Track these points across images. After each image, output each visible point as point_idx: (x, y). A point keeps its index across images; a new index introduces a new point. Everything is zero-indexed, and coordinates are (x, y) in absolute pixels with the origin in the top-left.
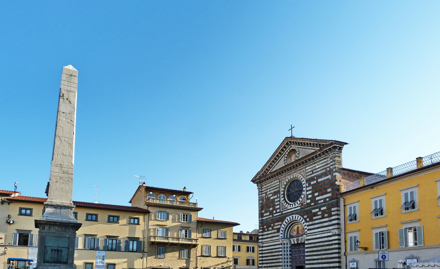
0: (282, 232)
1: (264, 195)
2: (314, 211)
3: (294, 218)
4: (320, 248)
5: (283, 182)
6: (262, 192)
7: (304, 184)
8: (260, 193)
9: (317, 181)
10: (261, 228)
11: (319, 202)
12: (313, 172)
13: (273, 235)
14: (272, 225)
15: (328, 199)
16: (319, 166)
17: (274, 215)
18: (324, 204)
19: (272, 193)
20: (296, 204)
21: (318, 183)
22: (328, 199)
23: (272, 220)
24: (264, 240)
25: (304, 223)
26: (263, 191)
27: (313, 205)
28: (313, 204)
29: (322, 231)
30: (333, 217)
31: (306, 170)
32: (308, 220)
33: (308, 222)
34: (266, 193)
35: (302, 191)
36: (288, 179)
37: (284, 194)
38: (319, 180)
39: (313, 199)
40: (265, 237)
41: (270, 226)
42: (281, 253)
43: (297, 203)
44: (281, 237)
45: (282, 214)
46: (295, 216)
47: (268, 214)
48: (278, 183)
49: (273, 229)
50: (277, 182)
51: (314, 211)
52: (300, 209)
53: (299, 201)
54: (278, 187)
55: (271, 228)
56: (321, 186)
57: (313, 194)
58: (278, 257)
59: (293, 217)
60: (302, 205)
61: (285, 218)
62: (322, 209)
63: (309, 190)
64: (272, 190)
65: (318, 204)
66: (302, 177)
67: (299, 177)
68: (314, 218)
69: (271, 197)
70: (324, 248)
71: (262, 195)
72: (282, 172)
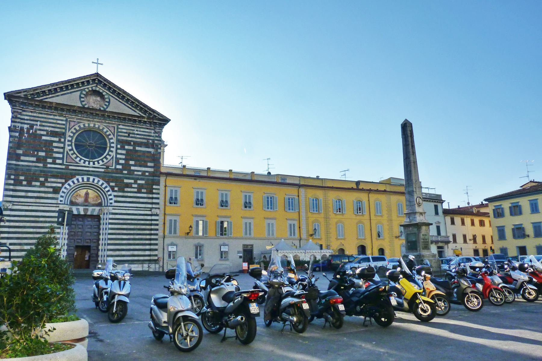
0: (63, 195)
1: (26, 126)
4: (132, 227)
5: (72, 124)
8: (14, 119)
9: (134, 148)
10: (12, 177)
11: (136, 173)
12: (129, 135)
15: (147, 174)
16: (140, 132)
17: (49, 166)
18: (142, 177)
20: (96, 163)
22: (147, 174)
23: (41, 171)
25: (109, 191)
27: (126, 174)
28: (125, 172)
30: (155, 196)
31: (118, 128)
33: (116, 191)
34: (32, 126)
36: (84, 125)
38: (137, 148)
40: (23, 194)
43: (99, 163)
44: (61, 201)
45: (67, 168)
46: (94, 180)
47: (34, 159)
49: (42, 185)
52: (104, 172)
56: (139, 156)
59: (88, 179)
60: (107, 167)
61: (72, 176)
62: (139, 182)
64: (49, 127)
65: (133, 174)
68: (126, 189)
69: (44, 135)
70: (138, 227)
71: (23, 125)
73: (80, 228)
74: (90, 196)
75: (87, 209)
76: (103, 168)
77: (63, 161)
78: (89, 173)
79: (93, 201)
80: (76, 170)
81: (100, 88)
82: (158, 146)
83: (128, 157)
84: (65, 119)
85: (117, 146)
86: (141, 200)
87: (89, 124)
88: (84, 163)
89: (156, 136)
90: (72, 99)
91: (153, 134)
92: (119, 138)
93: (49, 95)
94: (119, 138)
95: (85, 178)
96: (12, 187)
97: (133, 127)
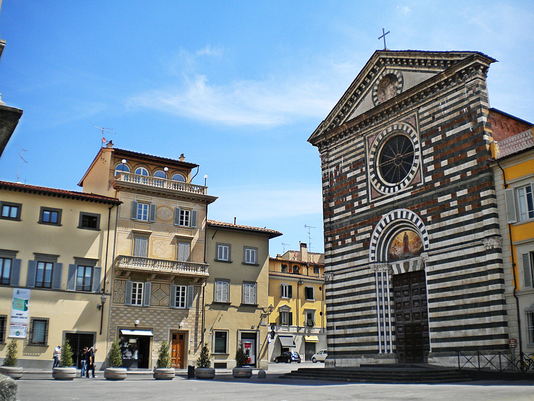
1: (333, 169)
2: (440, 199)
3: (399, 216)
4: (459, 282)
5: (371, 140)
6: (328, 162)
7: (416, 143)
8: (325, 165)
9: (444, 135)
10: (329, 239)
11: (452, 179)
12: (433, 118)
13: (355, 255)
14: (352, 233)
16: (446, 103)
17: (357, 211)
18: (462, 183)
19: (349, 165)
20: (402, 185)
21: (446, 139)
22: (469, 174)
23: (352, 222)
24: (335, 268)
25: (421, 225)
26: (332, 161)
27: (439, 187)
28: (438, 184)
29: (462, 243)
30: (485, 212)
32: (429, 219)
33: (429, 223)
34: (337, 165)
35: (411, 159)
36: (382, 134)
37: (374, 166)
38: (449, 134)
39: (438, 174)
40: (339, 259)
41: (349, 236)
42: (373, 295)
43: (404, 184)
45: (373, 208)
46: (402, 212)
47: (343, 209)
48: (362, 144)
49: (354, 242)
50: (360, 142)
51: (440, 199)
52: (411, 196)
53: (409, 179)
54: (363, 152)
55: (349, 240)
56: (453, 146)
57: (436, 162)
58: (368, 304)
59: (396, 214)
60: (415, 187)
61: (379, 217)
62: (459, 194)
63: (429, 155)
64: (350, 158)
65: (449, 183)
66: (411, 128)
67: (405, 129)
68: (444, 215)
70: (468, 281)
71: (329, 170)
72: (371, 121)
73: (406, 296)
74: (410, 240)
75: (408, 263)
76: (409, 190)
77: (368, 199)
78: (395, 205)
79: (414, 247)
80: (381, 206)
81: (390, 69)
82: (476, 112)
83: (437, 157)
84: (363, 138)
85: (421, 145)
86: (467, 228)
87: (387, 130)
88: (389, 192)
89: (471, 96)
90: (365, 105)
91: (466, 96)
92: (422, 129)
93: (344, 117)
94: (422, 129)
95: (392, 213)
96: (329, 253)
97: (436, 100)
